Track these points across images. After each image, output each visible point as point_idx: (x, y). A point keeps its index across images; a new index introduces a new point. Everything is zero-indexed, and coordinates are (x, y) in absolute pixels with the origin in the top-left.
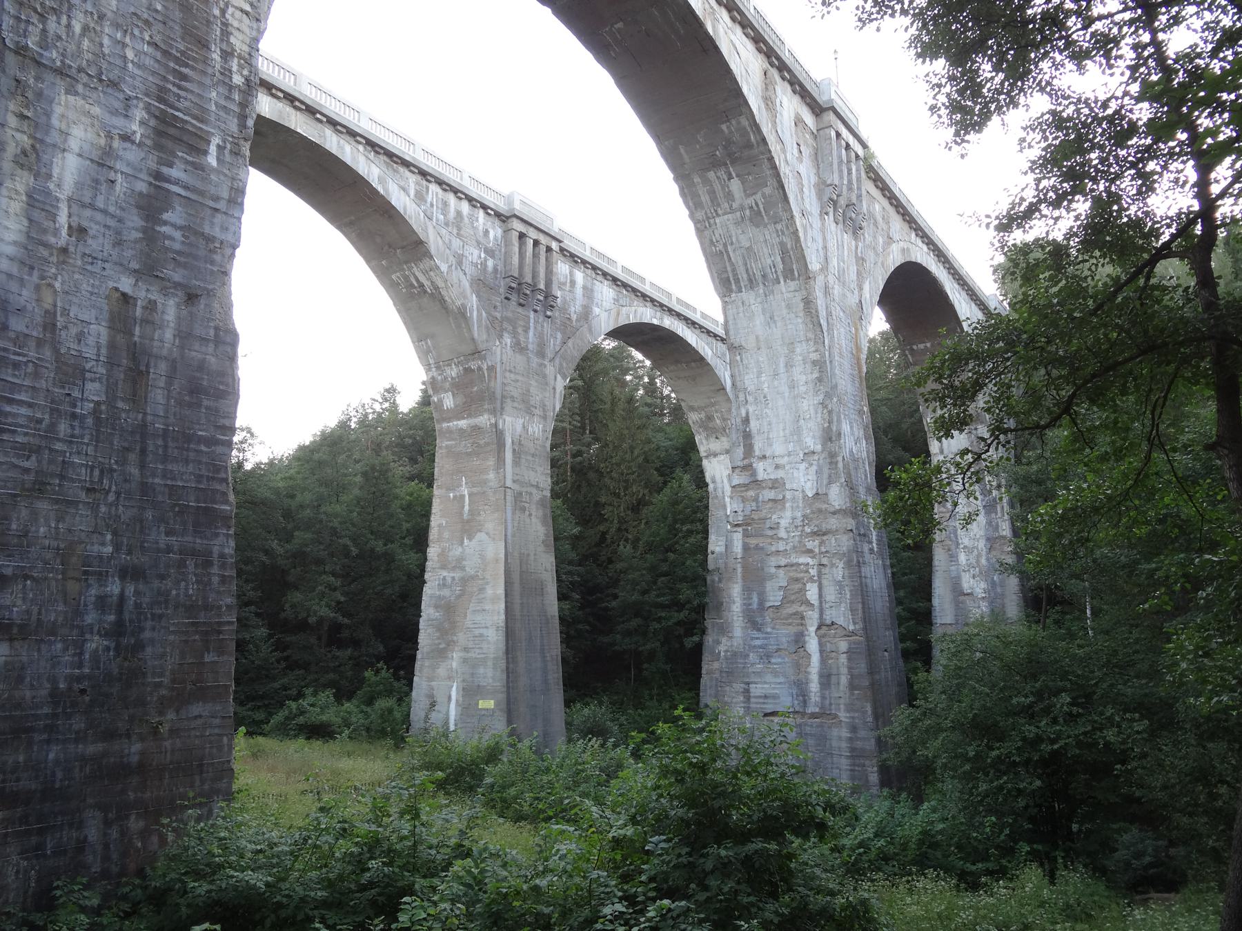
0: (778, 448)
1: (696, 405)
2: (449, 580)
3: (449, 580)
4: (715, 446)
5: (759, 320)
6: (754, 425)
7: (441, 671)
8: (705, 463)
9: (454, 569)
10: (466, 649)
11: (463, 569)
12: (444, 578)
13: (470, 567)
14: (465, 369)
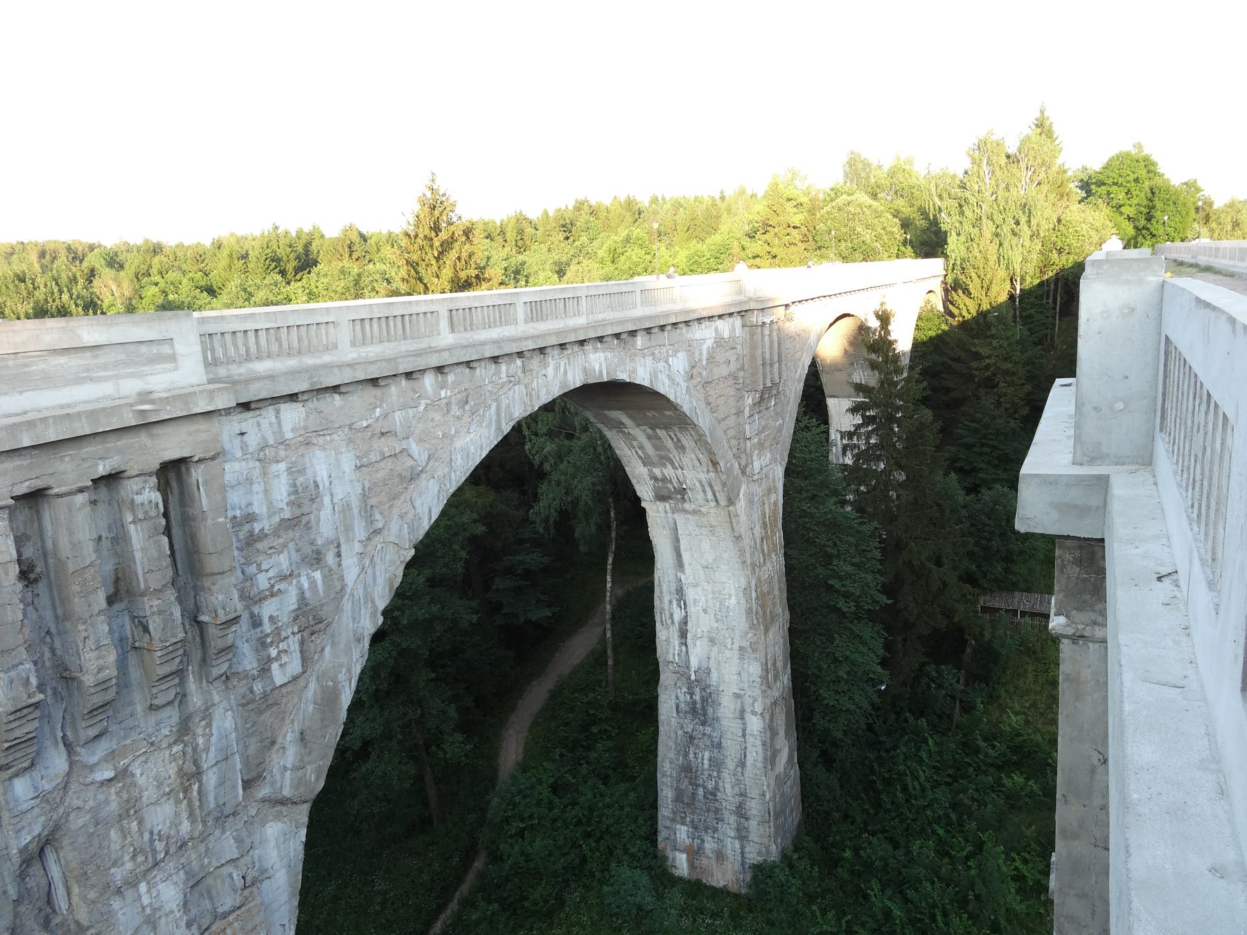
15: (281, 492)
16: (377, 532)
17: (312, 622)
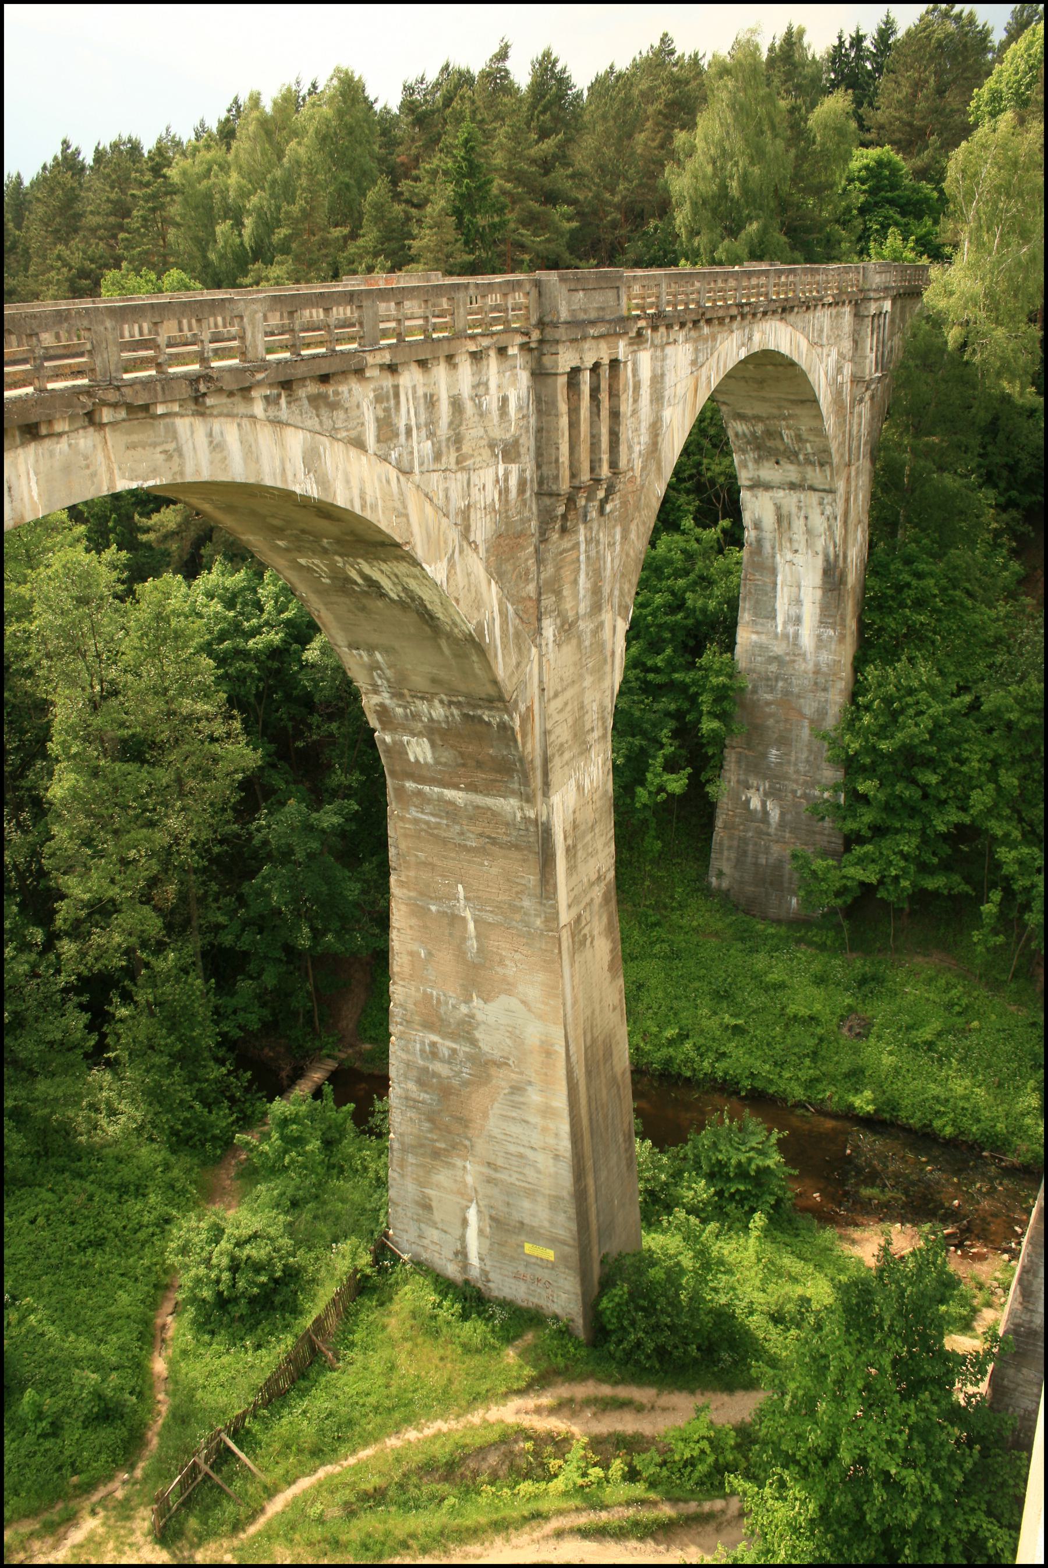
1: (749, 412)
4: (769, 472)
8: (745, 495)
9: (453, 1036)
11: (473, 1042)
12: (433, 1044)
13: (489, 1042)
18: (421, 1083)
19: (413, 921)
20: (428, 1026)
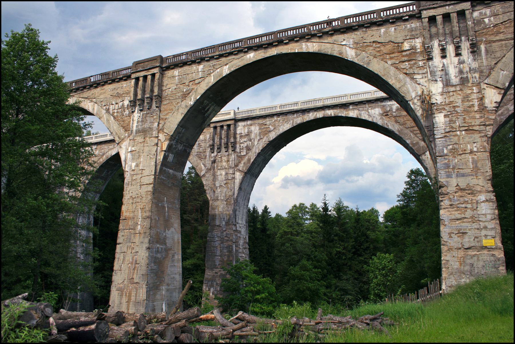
0: (240, 222)
2: (160, 249)
3: (160, 249)
5: (247, 184)
6: (237, 212)
7: (158, 297)
9: (161, 244)
10: (168, 285)
11: (165, 244)
12: (158, 247)
14: (185, 149)
15: (246, 131)
16: (262, 138)
17: (248, 149)
18: (155, 262)
19: (156, 209)
20: (158, 242)
